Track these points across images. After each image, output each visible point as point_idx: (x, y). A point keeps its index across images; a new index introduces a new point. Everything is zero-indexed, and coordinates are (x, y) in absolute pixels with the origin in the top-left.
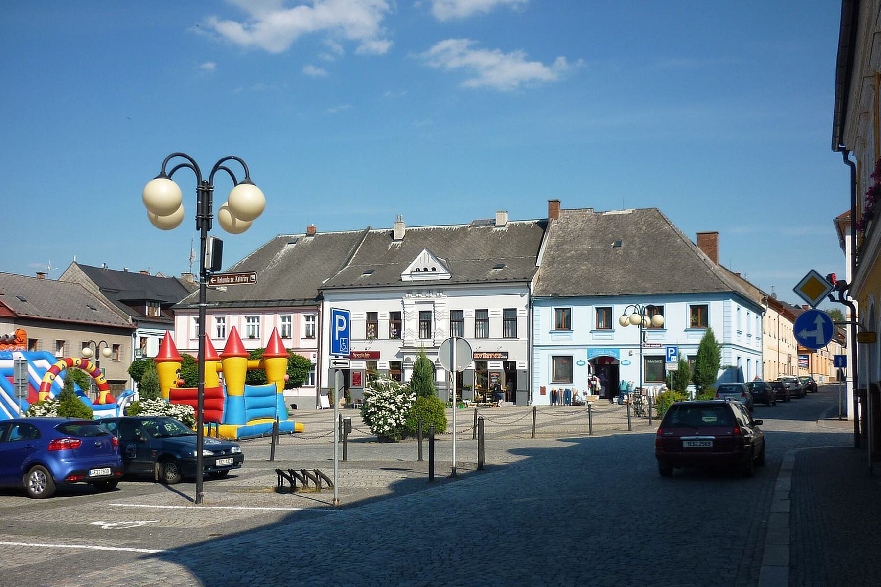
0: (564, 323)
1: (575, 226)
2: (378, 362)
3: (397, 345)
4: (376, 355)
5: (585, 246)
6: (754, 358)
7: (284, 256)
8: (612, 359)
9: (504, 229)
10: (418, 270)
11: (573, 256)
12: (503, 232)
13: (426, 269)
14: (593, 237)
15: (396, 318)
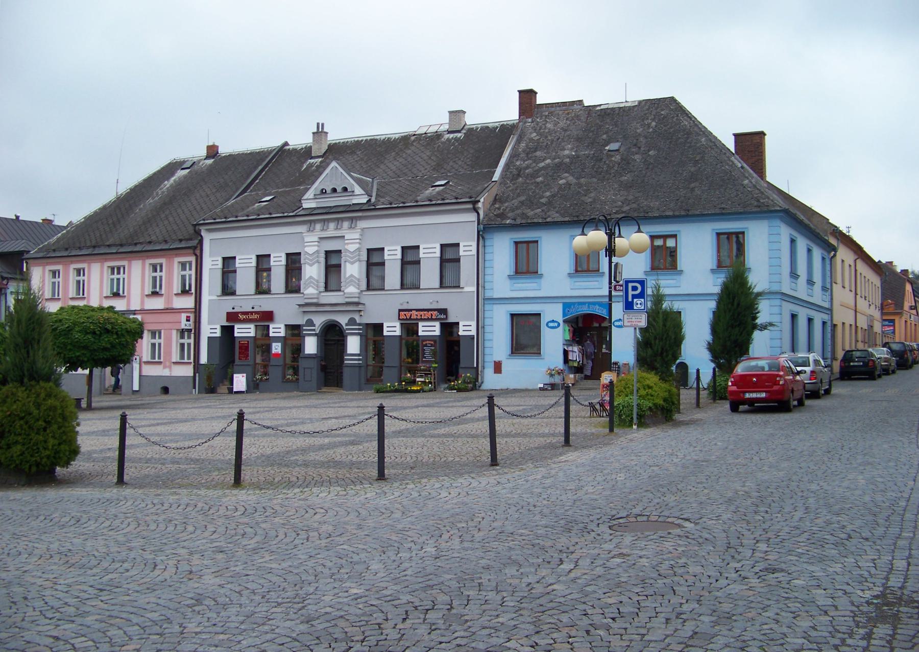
0: (526, 265)
1: (555, 125)
2: (271, 326)
3: (295, 299)
4: (268, 316)
5: (567, 152)
6: (818, 318)
7: (171, 186)
8: (601, 319)
9: (459, 135)
10: (323, 192)
11: (548, 166)
12: (456, 139)
13: (334, 190)
14: (578, 139)
15: (294, 263)
